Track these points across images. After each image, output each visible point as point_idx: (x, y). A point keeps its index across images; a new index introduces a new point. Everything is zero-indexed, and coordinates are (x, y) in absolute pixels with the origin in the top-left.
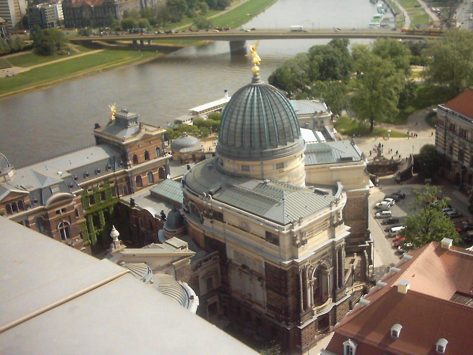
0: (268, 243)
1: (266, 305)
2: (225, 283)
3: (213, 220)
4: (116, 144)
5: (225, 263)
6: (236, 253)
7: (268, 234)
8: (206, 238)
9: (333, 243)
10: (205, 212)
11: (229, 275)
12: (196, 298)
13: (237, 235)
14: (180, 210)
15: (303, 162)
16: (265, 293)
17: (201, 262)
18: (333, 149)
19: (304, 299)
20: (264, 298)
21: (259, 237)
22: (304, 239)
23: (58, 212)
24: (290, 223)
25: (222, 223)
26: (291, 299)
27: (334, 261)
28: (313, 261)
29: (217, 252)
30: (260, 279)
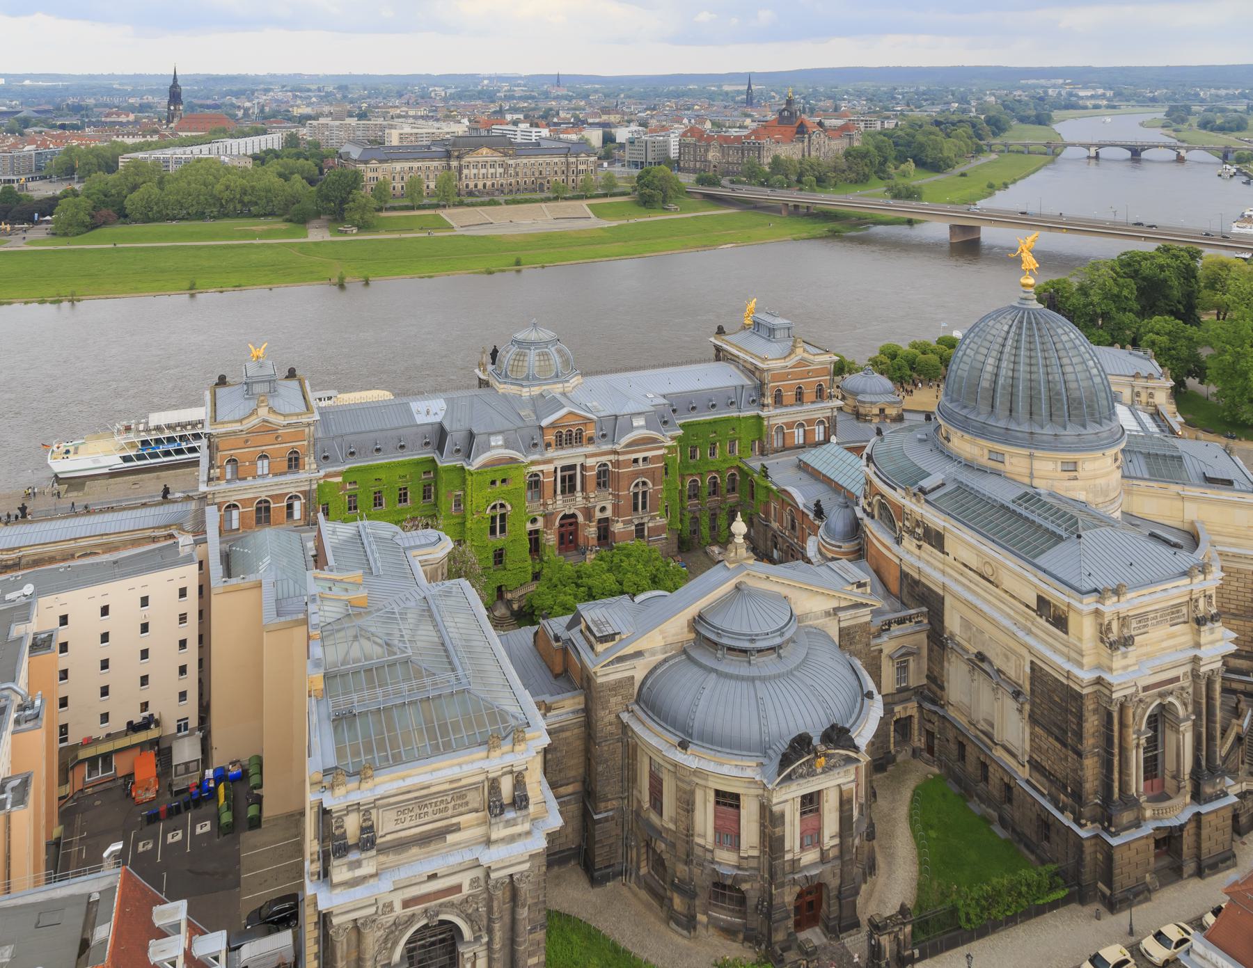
2: (936, 681)
4: (749, 366)
5: (938, 639)
6: (966, 624)
7: (1040, 599)
8: (904, 576)
9: (1196, 660)
12: (878, 697)
15: (1118, 468)
17: (889, 623)
18: (1186, 456)
19: (1121, 772)
22: (1126, 632)
23: (636, 461)
24: (1096, 590)
26: (1091, 768)
27: (1196, 703)
28: (1146, 689)
29: (925, 609)
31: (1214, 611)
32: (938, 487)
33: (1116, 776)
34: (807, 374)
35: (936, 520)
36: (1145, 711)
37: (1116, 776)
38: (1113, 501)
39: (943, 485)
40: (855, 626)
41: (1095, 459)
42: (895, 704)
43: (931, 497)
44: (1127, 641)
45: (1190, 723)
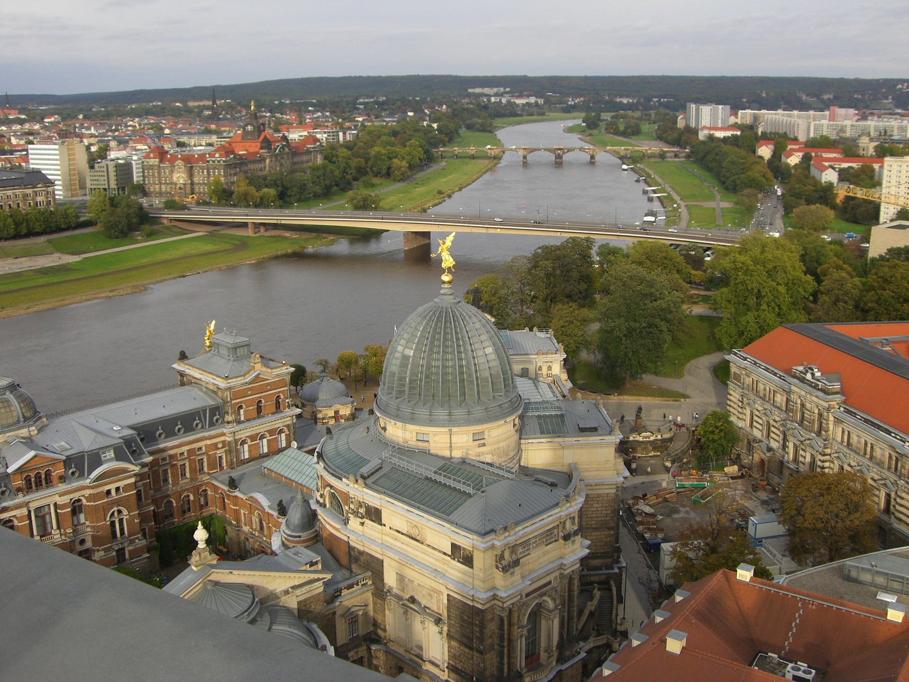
0: (455, 563)
1: (446, 665)
3: (364, 520)
4: (211, 387)
7: (454, 546)
10: (352, 506)
11: (387, 612)
13: (404, 547)
14: (311, 502)
16: (446, 645)
19: (509, 657)
20: (443, 653)
21: (440, 551)
23: (109, 492)
25: (380, 527)
28: (527, 595)
29: (369, 574)
30: (438, 621)
31: (576, 528)
32: (377, 471)
33: (506, 660)
34: (262, 389)
35: (373, 498)
36: (526, 610)
37: (506, 660)
38: (512, 459)
39: (381, 468)
40: (310, 598)
41: (499, 426)
42: (350, 651)
43: (369, 481)
44: (516, 563)
45: (557, 611)
